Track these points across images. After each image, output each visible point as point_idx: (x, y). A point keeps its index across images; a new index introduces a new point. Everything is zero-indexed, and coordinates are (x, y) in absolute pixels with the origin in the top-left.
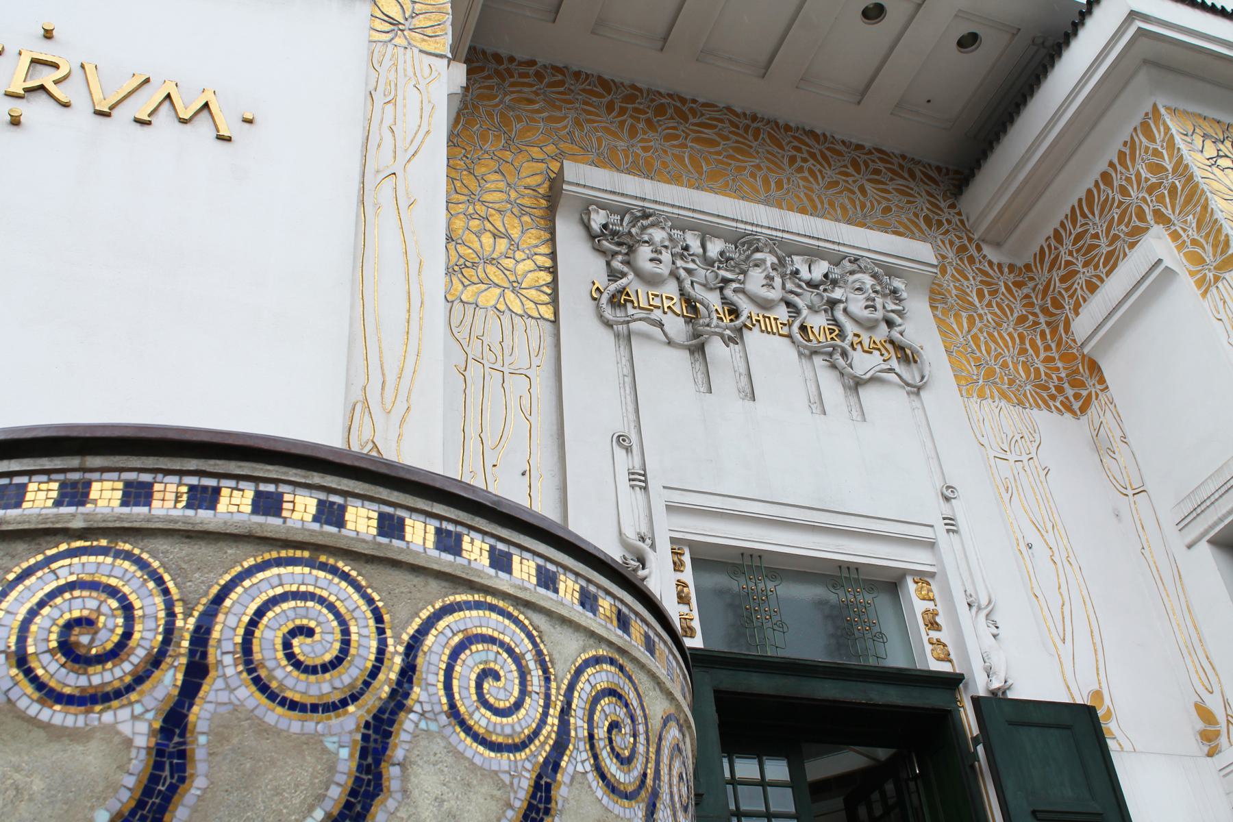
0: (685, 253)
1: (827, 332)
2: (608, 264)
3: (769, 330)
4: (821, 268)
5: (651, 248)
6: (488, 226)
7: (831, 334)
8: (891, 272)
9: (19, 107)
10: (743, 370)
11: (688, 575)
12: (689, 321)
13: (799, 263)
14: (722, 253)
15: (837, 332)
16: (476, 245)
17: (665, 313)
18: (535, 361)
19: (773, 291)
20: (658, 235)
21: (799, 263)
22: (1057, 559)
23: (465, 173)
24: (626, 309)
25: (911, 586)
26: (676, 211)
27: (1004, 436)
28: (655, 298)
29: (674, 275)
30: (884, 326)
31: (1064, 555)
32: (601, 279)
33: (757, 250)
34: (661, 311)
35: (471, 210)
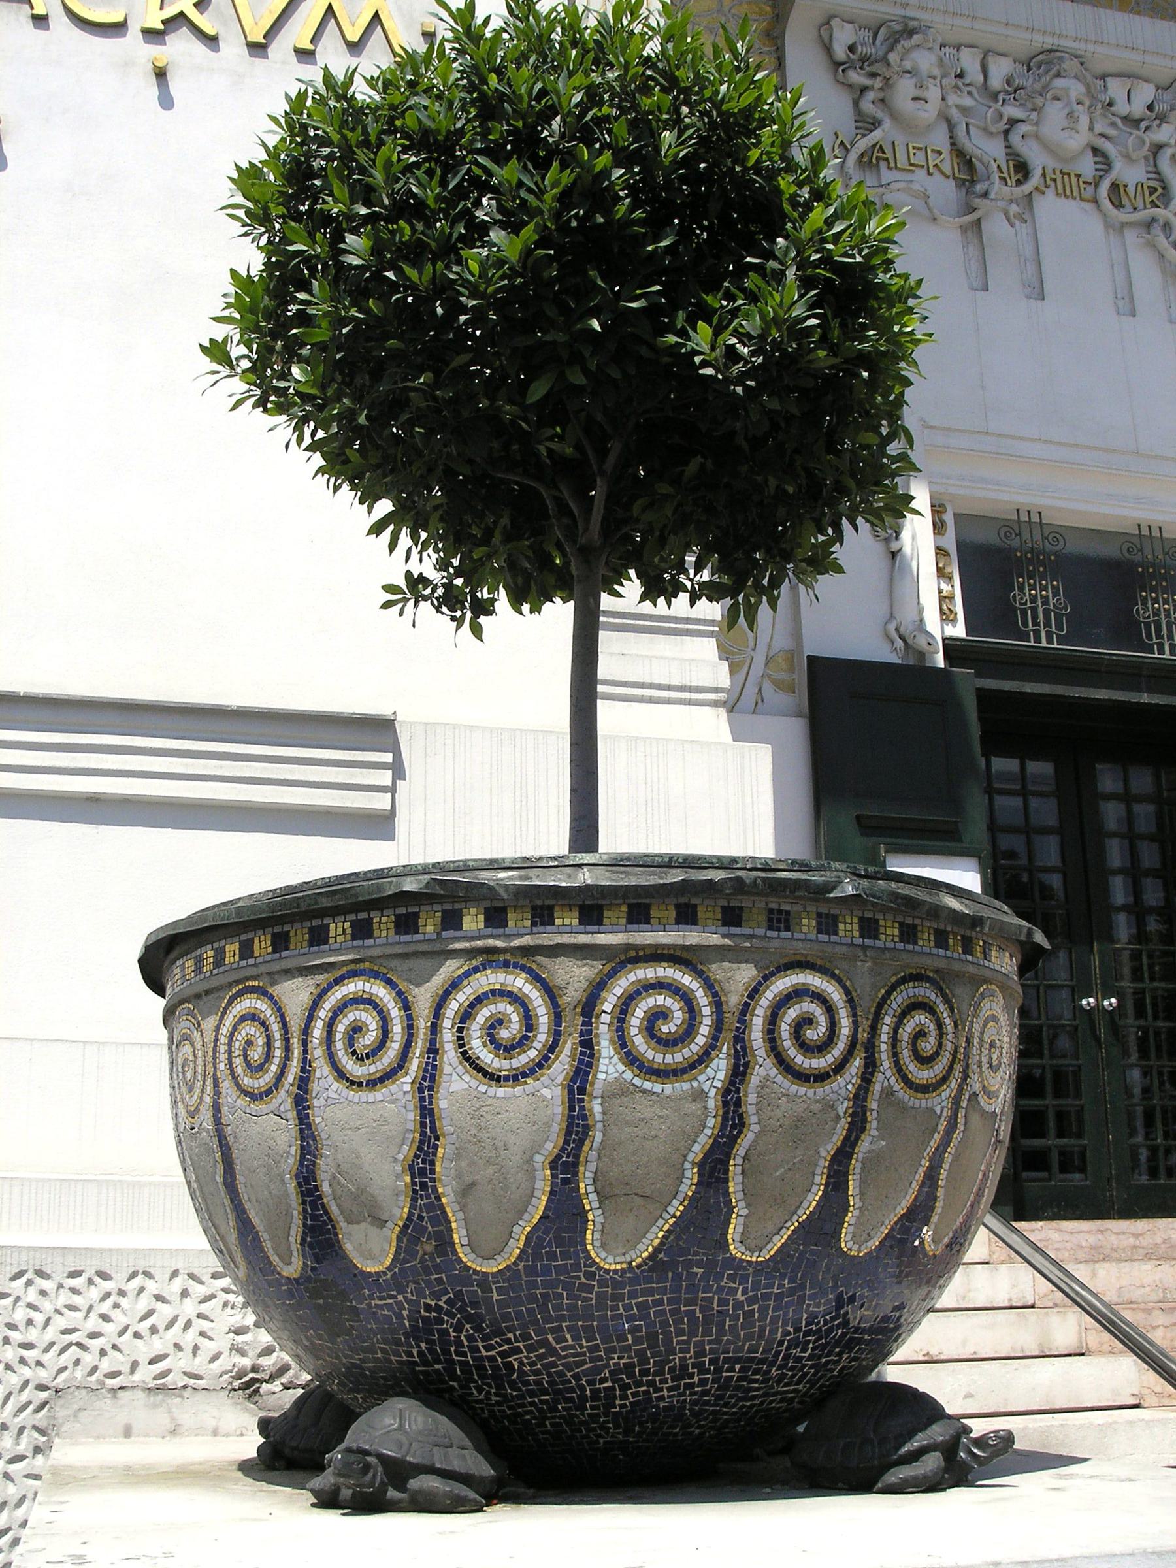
0: (960, 82)
1: (1147, 192)
2: (856, 103)
3: (1068, 193)
5: (914, 80)
7: (1151, 194)
10: (1029, 251)
11: (950, 541)
12: (960, 183)
13: (1116, 89)
15: (1160, 191)
17: (929, 174)
20: (925, 61)
24: (879, 171)
28: (918, 153)
34: (924, 171)
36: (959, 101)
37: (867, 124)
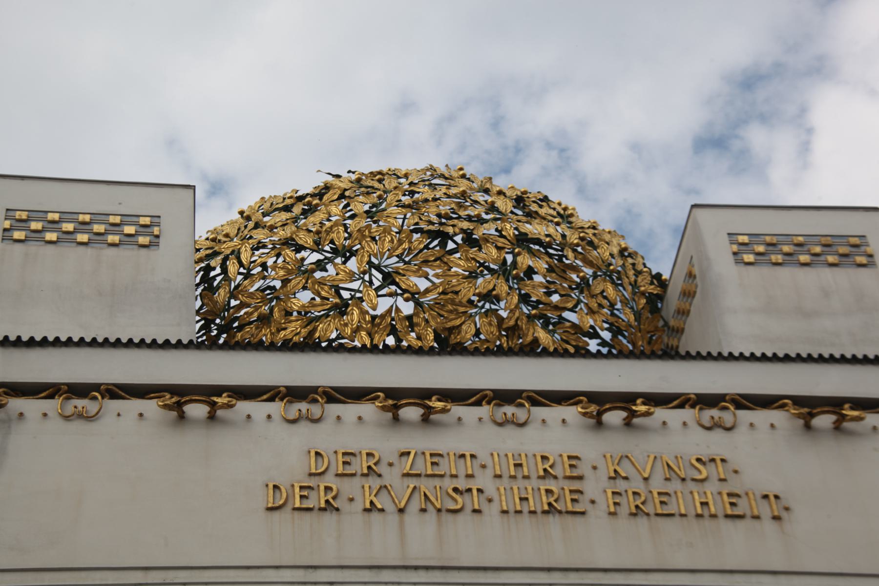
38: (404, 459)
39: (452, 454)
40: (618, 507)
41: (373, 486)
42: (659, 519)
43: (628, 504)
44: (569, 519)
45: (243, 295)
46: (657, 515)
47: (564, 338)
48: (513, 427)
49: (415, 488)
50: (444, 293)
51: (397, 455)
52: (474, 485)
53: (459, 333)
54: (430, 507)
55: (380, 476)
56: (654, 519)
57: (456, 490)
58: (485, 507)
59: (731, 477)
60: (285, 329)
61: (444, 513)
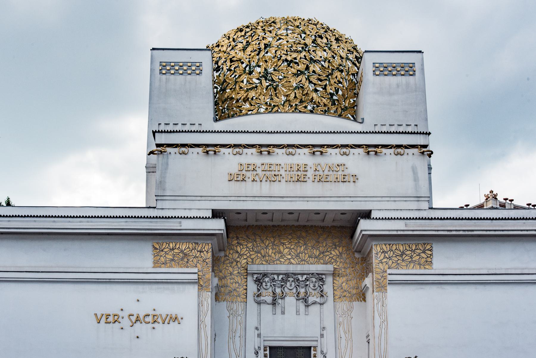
1: (304, 293)
2: (258, 286)
4: (305, 276)
6: (234, 281)
8: (322, 274)
9: (154, 325)
11: (268, 352)
14: (282, 278)
16: (232, 287)
18: (243, 312)
19: (292, 287)
20: (267, 279)
21: (300, 277)
22: (347, 340)
23: (230, 267)
25: (312, 349)
26: (271, 272)
27: (343, 311)
29: (271, 285)
30: (319, 287)
31: (349, 338)
32: (256, 290)
33: (289, 277)
35: (231, 278)
36: (274, 284)
37: (259, 290)
38: (263, 165)
39: (275, 164)
40: (315, 179)
41: (254, 174)
42: (325, 182)
43: (318, 178)
44: (302, 183)
45: (227, 80)
46: (324, 181)
47: (322, 95)
48: (291, 155)
49: (265, 174)
50: (286, 82)
51: (261, 165)
52: (279, 173)
53: (290, 96)
54: (268, 180)
55: (256, 171)
56: (323, 182)
57: (275, 175)
58: (282, 180)
59: (345, 170)
60: (240, 93)
61: (271, 182)
